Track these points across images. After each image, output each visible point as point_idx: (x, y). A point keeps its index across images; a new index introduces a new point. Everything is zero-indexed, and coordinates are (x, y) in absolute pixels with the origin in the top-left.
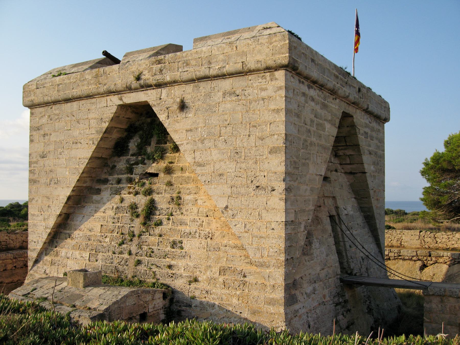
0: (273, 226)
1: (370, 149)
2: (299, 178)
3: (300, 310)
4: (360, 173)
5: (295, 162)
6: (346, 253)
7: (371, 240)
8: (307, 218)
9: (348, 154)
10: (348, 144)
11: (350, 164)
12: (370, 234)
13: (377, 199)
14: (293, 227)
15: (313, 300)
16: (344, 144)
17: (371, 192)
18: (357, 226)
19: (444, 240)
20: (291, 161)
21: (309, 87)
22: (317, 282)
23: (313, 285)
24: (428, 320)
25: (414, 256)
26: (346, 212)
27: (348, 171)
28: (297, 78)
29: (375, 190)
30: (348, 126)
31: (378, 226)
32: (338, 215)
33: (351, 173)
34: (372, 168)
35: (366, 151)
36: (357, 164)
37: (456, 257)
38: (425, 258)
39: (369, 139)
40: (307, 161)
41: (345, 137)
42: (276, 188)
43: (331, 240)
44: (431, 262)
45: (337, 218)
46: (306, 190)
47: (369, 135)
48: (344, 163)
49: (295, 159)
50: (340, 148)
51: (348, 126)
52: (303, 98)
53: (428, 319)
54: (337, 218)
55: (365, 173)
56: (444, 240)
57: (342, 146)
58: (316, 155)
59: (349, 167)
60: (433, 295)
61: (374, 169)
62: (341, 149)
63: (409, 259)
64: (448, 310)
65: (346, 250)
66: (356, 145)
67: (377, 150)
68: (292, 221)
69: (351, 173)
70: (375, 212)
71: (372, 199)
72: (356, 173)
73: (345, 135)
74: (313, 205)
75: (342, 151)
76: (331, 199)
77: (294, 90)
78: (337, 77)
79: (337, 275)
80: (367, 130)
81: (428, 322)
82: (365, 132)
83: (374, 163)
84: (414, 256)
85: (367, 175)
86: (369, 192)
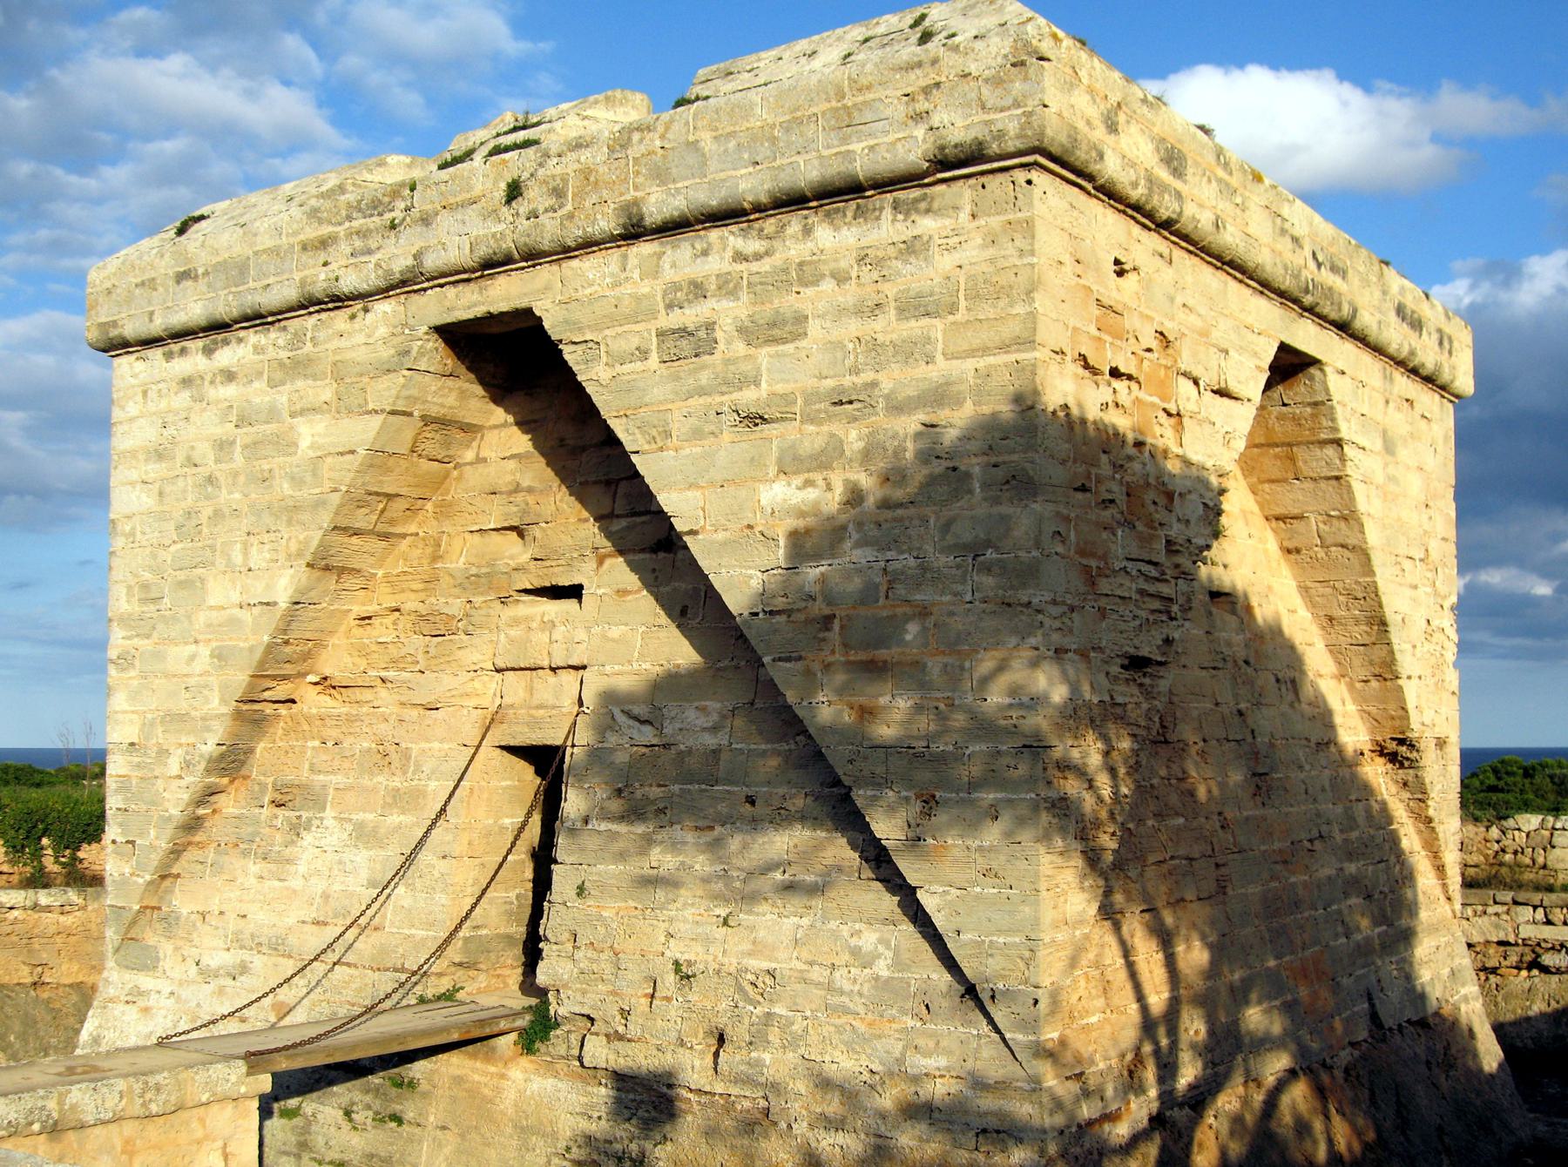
1: (748, 398)
3: (154, 996)
5: (145, 587)
14: (137, 760)
15: (221, 991)
20: (129, 588)
21: (208, 351)
23: (245, 955)
28: (156, 354)
40: (199, 571)
46: (192, 658)
49: (147, 576)
52: (186, 394)
68: (132, 744)
74: (223, 701)
77: (145, 393)
78: (324, 243)
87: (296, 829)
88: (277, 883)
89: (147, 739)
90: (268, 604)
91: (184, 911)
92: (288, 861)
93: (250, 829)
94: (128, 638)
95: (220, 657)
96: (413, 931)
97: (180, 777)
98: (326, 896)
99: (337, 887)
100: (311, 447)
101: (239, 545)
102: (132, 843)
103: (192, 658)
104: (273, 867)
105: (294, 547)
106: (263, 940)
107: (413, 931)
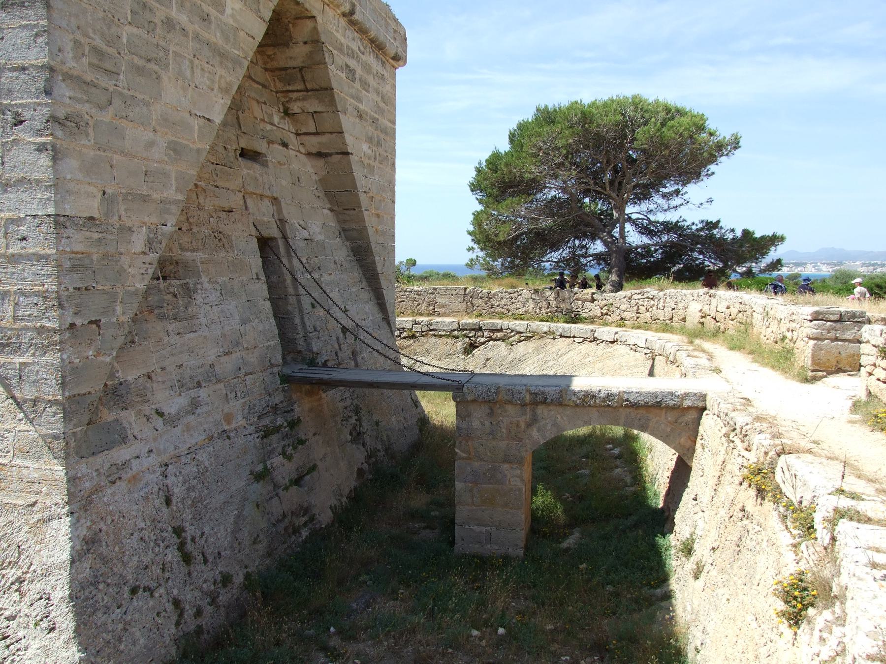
0: (23, 230)
1: (362, 107)
2: (117, 102)
3: (135, 463)
4: (337, 153)
6: (302, 319)
7: (366, 295)
8: (154, 220)
9: (311, 110)
10: (309, 86)
11: (316, 134)
12: (364, 284)
13: (378, 216)
14: (96, 236)
15: (188, 428)
16: (300, 86)
17: (363, 197)
18: (332, 266)
19: (503, 302)
20: (77, 44)
22: (203, 384)
23: (193, 393)
24: (464, 455)
25: (455, 330)
26: (305, 234)
27: (314, 151)
29: (371, 194)
30: (305, 43)
31: (379, 269)
32: (285, 237)
33: (320, 155)
34: (365, 147)
35: (350, 109)
36: (331, 133)
37: (522, 330)
38: (472, 333)
39: (357, 85)
40: (153, 66)
41: (301, 69)
42: (27, 114)
43: (261, 289)
44: (482, 340)
45: (281, 243)
46: (151, 144)
47: (357, 76)
48: (304, 131)
50: (294, 96)
51: (305, 43)
53: (462, 451)
54: (281, 243)
55: (347, 154)
56: (503, 302)
57: (298, 91)
58: (191, 62)
59: (314, 140)
60: (474, 401)
61: (369, 151)
62: (297, 100)
63: (448, 336)
64: (504, 430)
65: (301, 313)
66: (326, 89)
67: (377, 116)
68: (92, 218)
69: (320, 155)
70: (372, 239)
71: (365, 213)
72: (330, 155)
73: (301, 65)
74: (178, 189)
75: (299, 104)
76: (267, 202)
79: (272, 366)
80: (352, 63)
81: (463, 458)
82: (347, 66)
83: (370, 140)
84: (455, 330)
85: (353, 159)
86: (357, 196)
87: (189, 292)
88: (192, 335)
89: (108, 214)
90: (209, 120)
91: (130, 378)
92: (193, 317)
93: (156, 298)
94: (79, 101)
95: (175, 150)
96: (269, 343)
97: (144, 253)
98: (224, 335)
99: (227, 328)
100: (233, 16)
101: (187, 63)
102: (97, 322)
103: (151, 144)
104: (185, 323)
105: (223, 85)
106: (200, 378)
107: (269, 343)
